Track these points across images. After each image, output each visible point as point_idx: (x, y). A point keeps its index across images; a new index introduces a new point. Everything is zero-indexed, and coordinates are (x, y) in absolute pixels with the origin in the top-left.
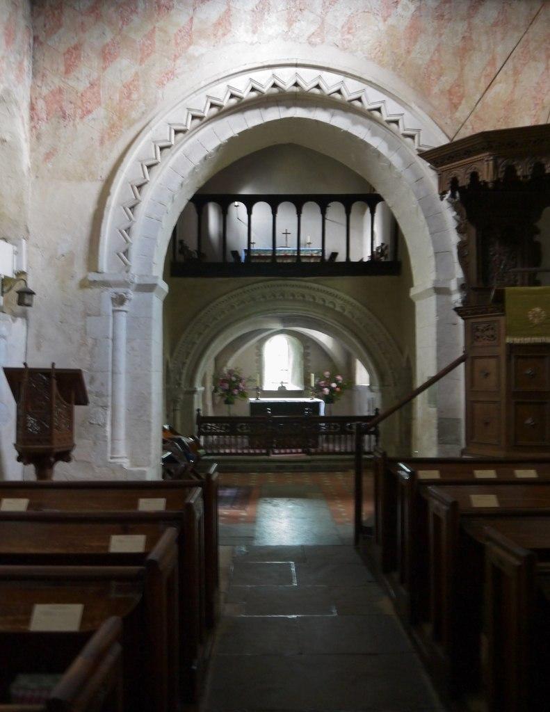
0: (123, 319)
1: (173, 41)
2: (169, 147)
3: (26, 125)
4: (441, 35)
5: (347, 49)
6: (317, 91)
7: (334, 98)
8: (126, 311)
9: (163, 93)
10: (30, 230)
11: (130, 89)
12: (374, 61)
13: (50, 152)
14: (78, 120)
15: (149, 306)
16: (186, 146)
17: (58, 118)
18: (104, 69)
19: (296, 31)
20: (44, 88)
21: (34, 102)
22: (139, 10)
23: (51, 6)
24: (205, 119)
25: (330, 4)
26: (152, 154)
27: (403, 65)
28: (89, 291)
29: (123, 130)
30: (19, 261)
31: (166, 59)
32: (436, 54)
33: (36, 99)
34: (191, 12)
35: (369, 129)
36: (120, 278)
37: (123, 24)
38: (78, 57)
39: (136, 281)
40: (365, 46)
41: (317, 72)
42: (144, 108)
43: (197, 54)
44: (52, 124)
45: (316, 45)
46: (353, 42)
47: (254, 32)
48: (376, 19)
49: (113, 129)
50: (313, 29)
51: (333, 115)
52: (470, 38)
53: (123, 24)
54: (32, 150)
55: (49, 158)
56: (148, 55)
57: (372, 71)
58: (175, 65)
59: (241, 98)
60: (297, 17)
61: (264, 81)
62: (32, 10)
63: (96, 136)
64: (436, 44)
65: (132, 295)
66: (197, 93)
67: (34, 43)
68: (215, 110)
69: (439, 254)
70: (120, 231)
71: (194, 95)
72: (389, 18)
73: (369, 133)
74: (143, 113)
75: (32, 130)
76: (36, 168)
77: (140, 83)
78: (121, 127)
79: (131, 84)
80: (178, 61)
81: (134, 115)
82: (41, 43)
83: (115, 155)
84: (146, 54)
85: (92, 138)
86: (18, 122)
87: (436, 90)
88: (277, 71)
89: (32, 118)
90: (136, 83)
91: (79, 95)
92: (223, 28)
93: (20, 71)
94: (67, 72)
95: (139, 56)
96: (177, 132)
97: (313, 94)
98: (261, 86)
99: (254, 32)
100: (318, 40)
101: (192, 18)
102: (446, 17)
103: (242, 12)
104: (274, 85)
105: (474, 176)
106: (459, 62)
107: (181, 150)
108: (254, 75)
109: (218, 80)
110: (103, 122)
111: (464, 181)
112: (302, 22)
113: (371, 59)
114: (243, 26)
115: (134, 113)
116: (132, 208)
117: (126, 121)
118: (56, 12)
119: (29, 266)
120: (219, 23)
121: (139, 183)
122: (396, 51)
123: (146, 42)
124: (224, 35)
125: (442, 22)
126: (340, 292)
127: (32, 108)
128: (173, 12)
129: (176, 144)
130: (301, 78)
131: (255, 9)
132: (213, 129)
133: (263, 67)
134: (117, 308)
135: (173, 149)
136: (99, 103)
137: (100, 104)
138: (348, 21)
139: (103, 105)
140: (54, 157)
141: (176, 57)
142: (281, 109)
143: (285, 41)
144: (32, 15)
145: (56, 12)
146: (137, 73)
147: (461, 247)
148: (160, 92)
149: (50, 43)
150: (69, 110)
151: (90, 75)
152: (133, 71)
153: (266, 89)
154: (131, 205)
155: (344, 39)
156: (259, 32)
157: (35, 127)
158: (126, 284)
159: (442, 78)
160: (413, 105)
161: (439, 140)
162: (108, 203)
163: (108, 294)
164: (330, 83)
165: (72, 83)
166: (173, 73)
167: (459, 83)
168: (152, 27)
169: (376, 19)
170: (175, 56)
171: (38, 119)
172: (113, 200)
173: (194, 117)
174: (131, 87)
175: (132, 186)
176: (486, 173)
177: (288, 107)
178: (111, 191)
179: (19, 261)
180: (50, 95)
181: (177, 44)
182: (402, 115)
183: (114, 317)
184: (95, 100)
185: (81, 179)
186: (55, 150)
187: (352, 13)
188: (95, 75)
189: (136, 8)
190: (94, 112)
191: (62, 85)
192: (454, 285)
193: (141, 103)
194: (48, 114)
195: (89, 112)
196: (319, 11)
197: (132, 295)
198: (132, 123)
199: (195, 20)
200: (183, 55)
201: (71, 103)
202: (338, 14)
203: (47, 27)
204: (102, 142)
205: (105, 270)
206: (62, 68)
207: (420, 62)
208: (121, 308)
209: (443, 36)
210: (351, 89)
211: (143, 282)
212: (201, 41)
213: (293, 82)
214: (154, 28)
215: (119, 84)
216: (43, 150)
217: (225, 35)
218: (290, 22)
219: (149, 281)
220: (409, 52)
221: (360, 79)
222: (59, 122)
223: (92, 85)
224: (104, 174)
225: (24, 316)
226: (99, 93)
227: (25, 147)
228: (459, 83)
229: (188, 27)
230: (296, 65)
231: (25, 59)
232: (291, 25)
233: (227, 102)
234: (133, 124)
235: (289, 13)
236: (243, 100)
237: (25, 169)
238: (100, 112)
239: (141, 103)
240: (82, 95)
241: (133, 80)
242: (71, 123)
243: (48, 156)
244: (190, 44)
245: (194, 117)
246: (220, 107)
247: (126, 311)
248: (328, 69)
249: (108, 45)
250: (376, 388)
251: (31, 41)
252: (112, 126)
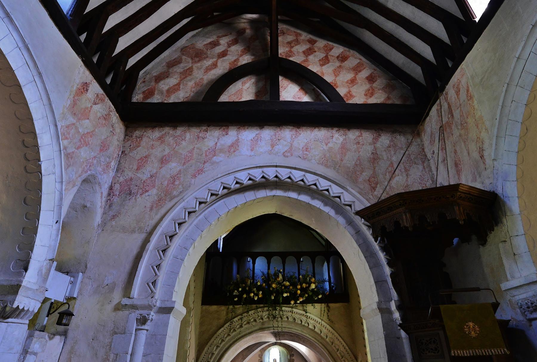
0: (143, 335)
1: (204, 155)
2: (194, 212)
3: (103, 197)
4: (359, 152)
5: (305, 159)
6: (289, 180)
7: (299, 184)
8: (147, 330)
9: (195, 181)
10: (88, 266)
11: (175, 179)
12: (322, 165)
13: (116, 215)
14: (138, 196)
15: (166, 325)
16: (206, 212)
17: (127, 194)
18: (161, 168)
19: (276, 150)
20: (121, 178)
21: (113, 185)
22: (187, 139)
23: (136, 137)
24: (219, 196)
25: (295, 137)
26: (183, 216)
27: (339, 166)
28: (120, 313)
29: (166, 202)
30: (72, 290)
31: (199, 163)
32: (358, 162)
33: (115, 183)
34: (216, 140)
35: (322, 202)
36: (145, 302)
37: (176, 146)
38: (147, 161)
39: (158, 304)
40: (316, 157)
41: (289, 170)
42: (181, 190)
43: (217, 161)
44: (121, 197)
45: (287, 157)
46: (309, 155)
47: (252, 150)
48: (322, 144)
49: (160, 202)
50: (286, 149)
51: (299, 194)
52: (376, 153)
53: (176, 146)
54: (104, 213)
55: (114, 218)
56: (189, 161)
57: (321, 170)
58: (204, 166)
59: (242, 184)
60: (276, 143)
61: (257, 175)
62: (125, 138)
63: (149, 205)
64: (357, 157)
65: (153, 315)
66: (215, 181)
67: (122, 154)
68: (226, 191)
69: (379, 282)
70: (152, 267)
71: (213, 182)
72: (329, 144)
73: (322, 204)
74: (181, 192)
75: (107, 202)
76: (103, 225)
77: (181, 175)
78: (165, 200)
79: (176, 176)
80: (206, 164)
81: (175, 193)
82: (126, 154)
83: (158, 217)
84: (187, 160)
85: (145, 207)
86: (98, 196)
87: (360, 180)
88: (265, 170)
89: (109, 195)
90: (179, 175)
91: (142, 181)
92: (235, 148)
93: (107, 167)
94: (138, 169)
95: (183, 162)
96: (200, 203)
97: (287, 182)
98: (255, 177)
99: (252, 150)
100: (289, 154)
101: (217, 143)
102: (361, 143)
103: (245, 140)
104: (263, 177)
106: (372, 165)
107: (203, 214)
108: (251, 172)
109: (229, 174)
110: (154, 197)
112: (279, 146)
113: (320, 163)
114: (245, 147)
115: (175, 192)
116: (164, 251)
117: (169, 196)
118: (138, 140)
119: (80, 293)
120: (232, 146)
121: (170, 235)
122: (334, 160)
123: (188, 154)
124: (234, 151)
125: (359, 146)
127: (111, 188)
128: (206, 140)
129: (199, 210)
130: (279, 173)
131: (253, 139)
132: (224, 202)
133: (257, 167)
134: (140, 327)
135: (197, 214)
136: (154, 186)
137: (154, 187)
138: (306, 145)
139: (156, 188)
140: (118, 218)
141: (205, 162)
142: (268, 191)
143: (270, 155)
144: (124, 141)
145: (138, 140)
146: (180, 171)
148: (193, 180)
149: (131, 154)
150: (134, 190)
151: (151, 171)
152: (178, 169)
153: (258, 179)
154: (163, 249)
155: (304, 154)
156: (254, 150)
157: (110, 200)
158: (149, 307)
159: (363, 173)
160: (348, 188)
162: (147, 247)
163: (135, 315)
164: (297, 176)
165: (139, 175)
166: (202, 170)
167: (374, 175)
168: (193, 147)
169: (322, 144)
170: (205, 161)
171: (113, 196)
172: (151, 246)
173: (212, 195)
174: (176, 178)
175: (166, 236)
177: (272, 189)
178: (151, 239)
179: (72, 290)
180: (124, 181)
181: (206, 155)
182: (342, 193)
183: (136, 335)
184: (152, 185)
185: (133, 231)
186: (120, 213)
187: (308, 142)
188: (155, 171)
189: (185, 138)
190: (150, 191)
191: (133, 176)
193: (180, 187)
194: (120, 192)
195: (147, 191)
196: (289, 140)
197: (153, 315)
198: (171, 199)
199: (218, 144)
200: (209, 161)
201: (136, 186)
202: (300, 142)
203: (131, 147)
204: (151, 209)
205: (135, 296)
206: (135, 167)
207: (349, 165)
208: (143, 327)
209: (360, 152)
210: (310, 179)
211: (163, 306)
212: (220, 154)
213: (275, 175)
214: (194, 147)
215: (169, 176)
216: (111, 213)
217: (235, 151)
218: (273, 146)
219: (168, 305)
220: (342, 160)
221: (315, 174)
222: (126, 197)
223: (152, 176)
224: (149, 229)
225: (65, 334)
226: (155, 181)
227: (99, 212)
228: (374, 175)
229: (214, 148)
230: (276, 166)
231: (113, 161)
232: (274, 147)
233: (233, 186)
234: (174, 198)
235: (272, 141)
236: (244, 185)
237: (96, 224)
238: (154, 191)
239: (180, 187)
240: (144, 182)
241: (177, 174)
242: (134, 198)
243: (114, 217)
244: (214, 156)
245: (212, 195)
246: (229, 189)
247: (147, 330)
248: (295, 169)
249: (165, 156)
251: (120, 153)
252: (160, 200)
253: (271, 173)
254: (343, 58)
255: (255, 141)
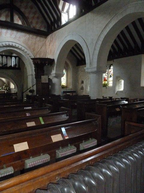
57: (23, 44)
61: (7, 44)
87: (31, 48)
99: (6, 35)
105: (38, 62)
108: (6, 43)
111: (36, 63)
126: (10, 72)
147: (35, 70)
161: (33, 57)
164: (17, 45)
176: (39, 62)
192: (34, 74)
210: (20, 47)
218: (11, 35)
250: (16, 88)
253: (11, 44)
254: (31, 8)
255: (6, 33)
